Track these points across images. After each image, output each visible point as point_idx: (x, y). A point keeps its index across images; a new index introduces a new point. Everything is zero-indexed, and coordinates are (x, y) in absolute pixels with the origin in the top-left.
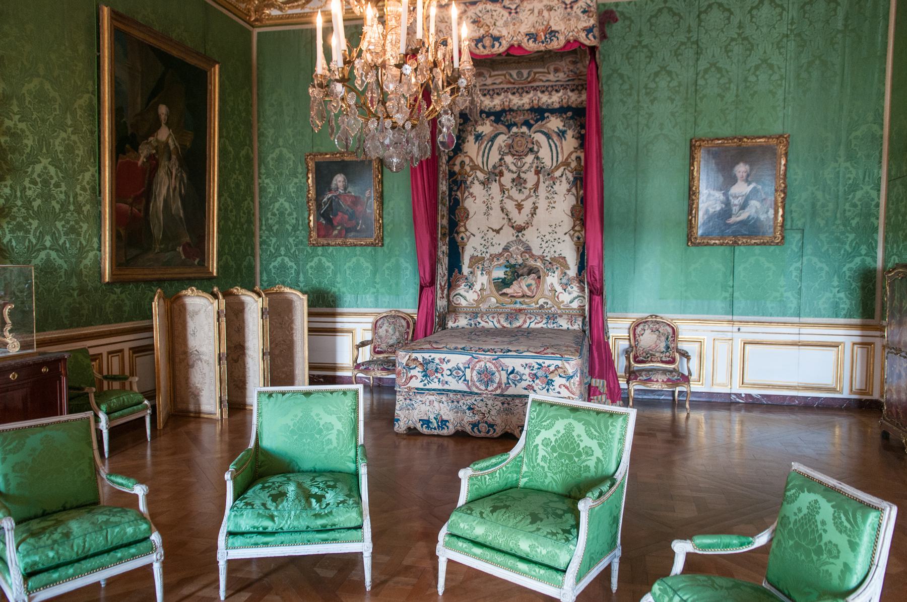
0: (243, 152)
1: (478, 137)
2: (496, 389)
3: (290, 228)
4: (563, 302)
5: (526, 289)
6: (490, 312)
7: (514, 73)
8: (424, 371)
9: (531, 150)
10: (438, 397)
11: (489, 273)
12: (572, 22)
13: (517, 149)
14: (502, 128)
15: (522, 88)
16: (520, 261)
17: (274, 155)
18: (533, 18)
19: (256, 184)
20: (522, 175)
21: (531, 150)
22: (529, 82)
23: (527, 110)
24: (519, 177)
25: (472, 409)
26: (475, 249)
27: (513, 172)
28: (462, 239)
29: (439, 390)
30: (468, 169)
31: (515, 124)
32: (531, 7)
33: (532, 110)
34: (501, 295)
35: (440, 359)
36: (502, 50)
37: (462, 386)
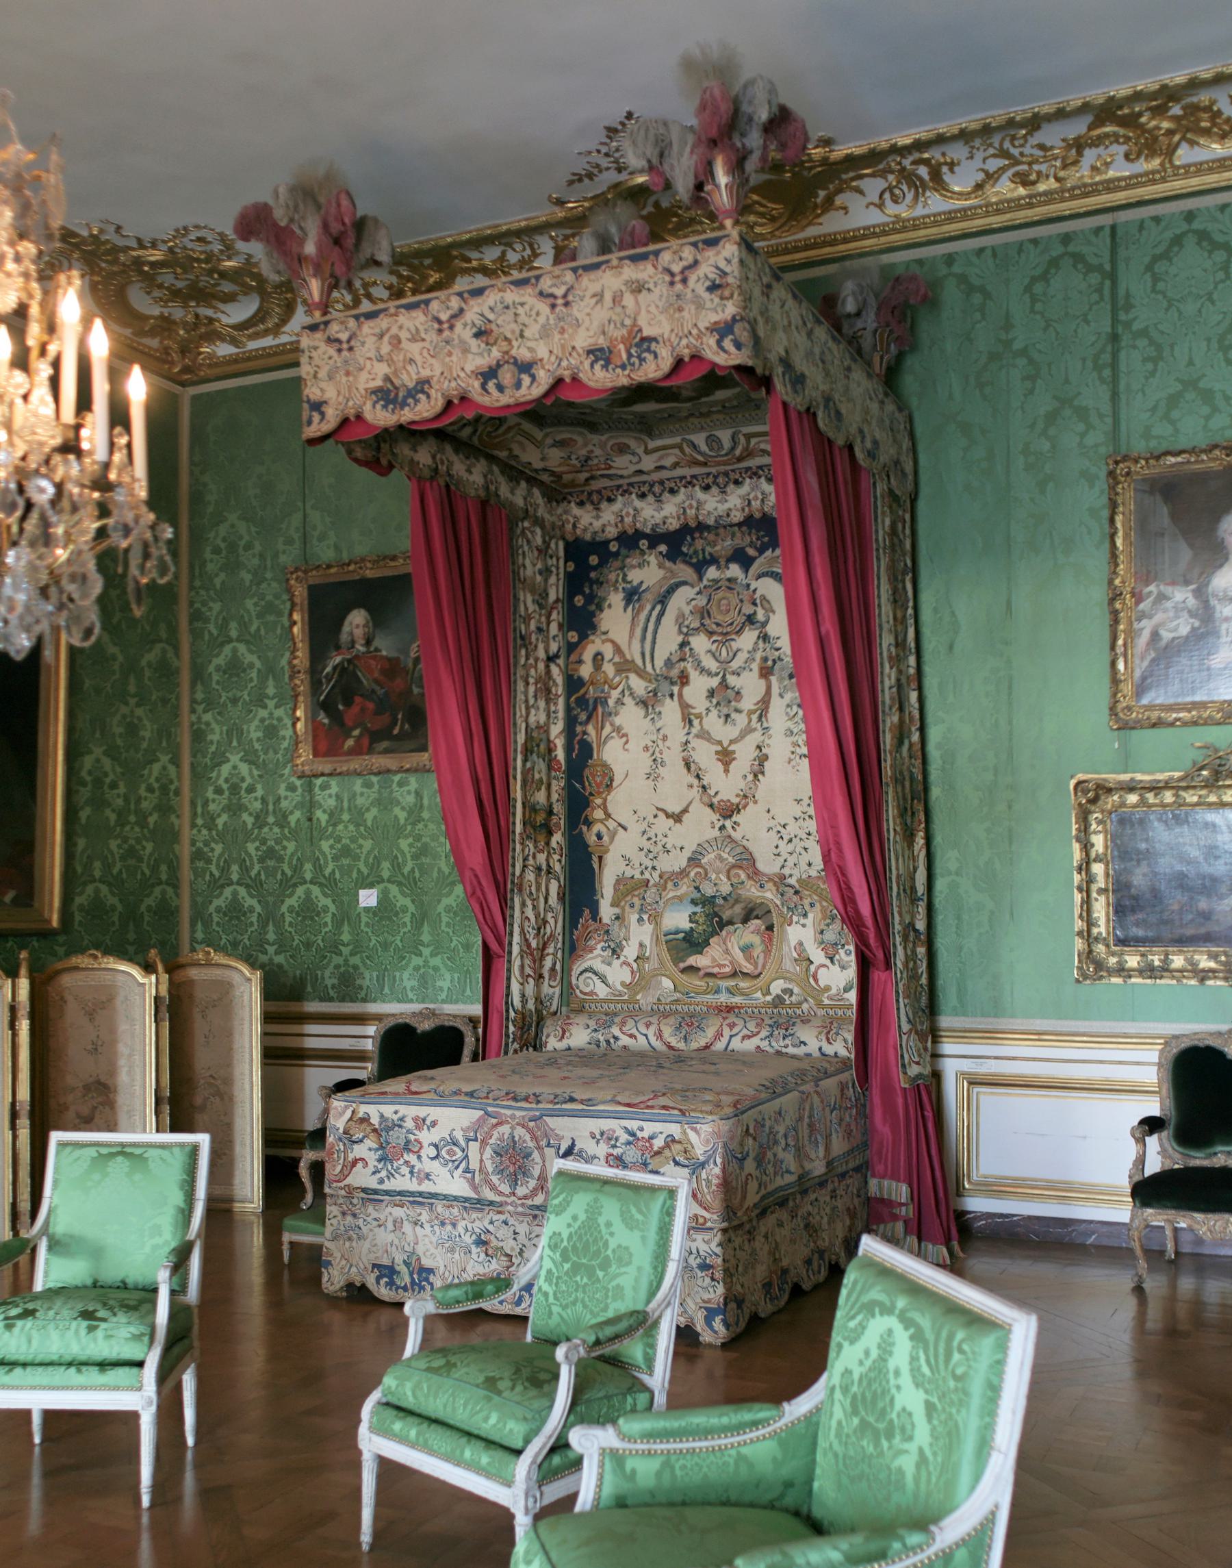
0: (151, 656)
1: (632, 595)
2: (534, 1193)
3: (250, 821)
4: (828, 988)
5: (739, 956)
6: (660, 1012)
7: (700, 439)
8: (381, 1147)
9: (751, 619)
10: (412, 1212)
11: (656, 919)
12: (685, 314)
13: (720, 618)
14: (684, 571)
15: (726, 474)
16: (725, 889)
17: (220, 661)
18: (602, 314)
19: (186, 724)
20: (732, 680)
21: (751, 619)
22: (740, 459)
23: (740, 525)
24: (724, 684)
25: (485, 1243)
26: (628, 861)
27: (709, 674)
28: (599, 837)
29: (412, 1194)
30: (609, 669)
31: (713, 561)
32: (595, 287)
33: (749, 522)
34: (683, 971)
35: (415, 1119)
36: (537, 392)
37: (457, 1186)
